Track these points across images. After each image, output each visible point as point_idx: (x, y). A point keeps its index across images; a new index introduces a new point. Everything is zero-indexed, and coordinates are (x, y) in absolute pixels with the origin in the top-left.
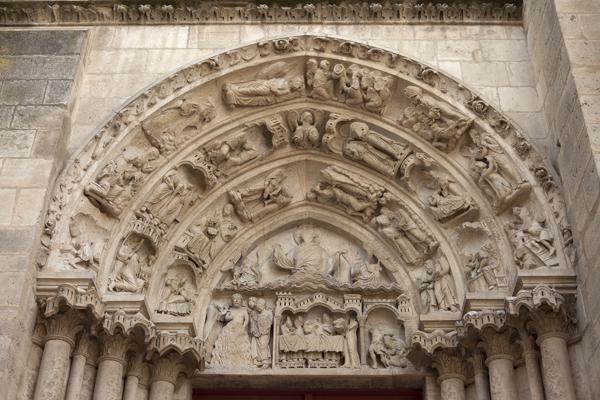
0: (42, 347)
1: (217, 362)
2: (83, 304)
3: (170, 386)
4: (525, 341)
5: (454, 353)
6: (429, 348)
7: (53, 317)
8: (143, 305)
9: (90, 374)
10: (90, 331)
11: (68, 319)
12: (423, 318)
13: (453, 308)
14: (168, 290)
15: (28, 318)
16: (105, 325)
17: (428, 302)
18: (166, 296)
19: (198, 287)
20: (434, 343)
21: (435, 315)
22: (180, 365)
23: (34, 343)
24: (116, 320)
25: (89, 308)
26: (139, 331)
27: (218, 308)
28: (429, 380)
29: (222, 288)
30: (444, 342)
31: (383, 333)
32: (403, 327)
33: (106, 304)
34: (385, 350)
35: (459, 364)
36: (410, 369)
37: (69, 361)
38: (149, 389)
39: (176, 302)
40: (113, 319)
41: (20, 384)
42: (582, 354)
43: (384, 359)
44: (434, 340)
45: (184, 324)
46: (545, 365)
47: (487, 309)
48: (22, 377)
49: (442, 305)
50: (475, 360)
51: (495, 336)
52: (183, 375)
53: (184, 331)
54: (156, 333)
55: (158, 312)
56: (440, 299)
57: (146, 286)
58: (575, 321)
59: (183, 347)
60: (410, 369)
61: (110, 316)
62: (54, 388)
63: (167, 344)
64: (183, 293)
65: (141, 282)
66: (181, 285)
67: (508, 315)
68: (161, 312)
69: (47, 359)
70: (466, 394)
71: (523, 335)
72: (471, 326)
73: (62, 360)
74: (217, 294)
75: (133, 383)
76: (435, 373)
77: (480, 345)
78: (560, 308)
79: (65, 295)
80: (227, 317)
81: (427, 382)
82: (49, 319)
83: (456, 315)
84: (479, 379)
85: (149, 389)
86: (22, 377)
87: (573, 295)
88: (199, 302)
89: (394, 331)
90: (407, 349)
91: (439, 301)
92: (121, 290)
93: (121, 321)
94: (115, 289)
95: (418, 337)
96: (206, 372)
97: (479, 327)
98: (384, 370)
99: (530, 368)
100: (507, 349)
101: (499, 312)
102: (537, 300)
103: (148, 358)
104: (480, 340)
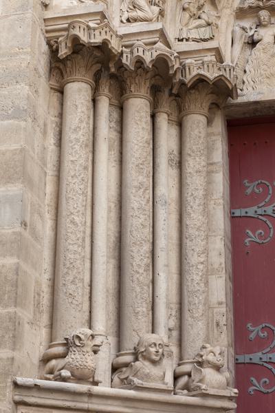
0: (61, 91)
1: (250, 89)
2: (97, 39)
3: (203, 119)
7: (67, 58)
8: (162, 34)
9: (115, 115)
10: (108, 69)
11: (83, 57)
14: (187, 15)
15: (41, 60)
16: (124, 61)
18: (185, 21)
19: (219, 8)
22: (207, 98)
23: (51, 88)
24: (136, 54)
25: (105, 43)
26: (162, 62)
27: (244, 29)
29: (246, 5)
33: (122, 37)
37: (90, 104)
38: (180, 125)
39: (197, 27)
40: (132, 52)
41: (45, 133)
45: (209, 50)
48: (45, 125)
52: (214, 106)
53: (210, 58)
54: (181, 64)
55: (179, 40)
57: (162, 13)
59: (212, 74)
61: (128, 50)
62: (80, 133)
63: (194, 73)
64: (203, 16)
65: (156, 9)
66: (199, 8)
68: (182, 40)
69: (69, 103)
73: (86, 103)
74: (241, 13)
75: (163, 120)
79: (76, 32)
80: (256, 37)
82: (64, 61)
85: (180, 125)
86: (45, 125)
88: (222, 24)
92: (135, 20)
93: (141, 54)
94: (128, 20)
96: (240, 100)
103: (175, 91)
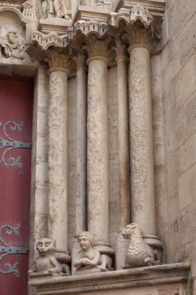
4: (119, 49)
5: (63, 51)
6: (44, 45)
12: (42, 21)
13: (66, 17)
17: (47, 10)
20: (49, 42)
21: (51, 20)
28: (40, 71)
30: (56, 42)
31: (8, 30)
32: (25, 28)
34: (9, 44)
35: (66, 61)
36: (27, 61)
42: (160, 63)
43: (7, 51)
44: (49, 40)
46: (132, 67)
47: (94, 20)
49: (58, 14)
50: (79, 59)
51: (97, 42)
56: (57, 9)
58: (159, 37)
60: (27, 61)
67: (110, 26)
70: (68, 84)
71: (118, 43)
72: (79, 32)
76: (46, 66)
77: (84, 47)
78: (150, 25)
81: (39, 72)
83: (68, 22)
84: (80, 74)
87: (161, 17)
89: (18, 31)
90: (26, 45)
91: (56, 10)
95: (37, 36)
97: (86, 33)
98: (6, 59)
99: (120, 69)
100: (104, 52)
101: (102, 23)
102: (133, 17)
104: (84, 44)
